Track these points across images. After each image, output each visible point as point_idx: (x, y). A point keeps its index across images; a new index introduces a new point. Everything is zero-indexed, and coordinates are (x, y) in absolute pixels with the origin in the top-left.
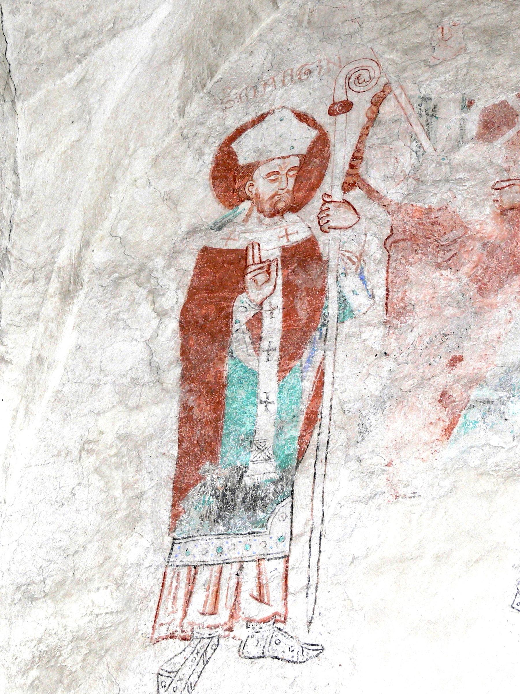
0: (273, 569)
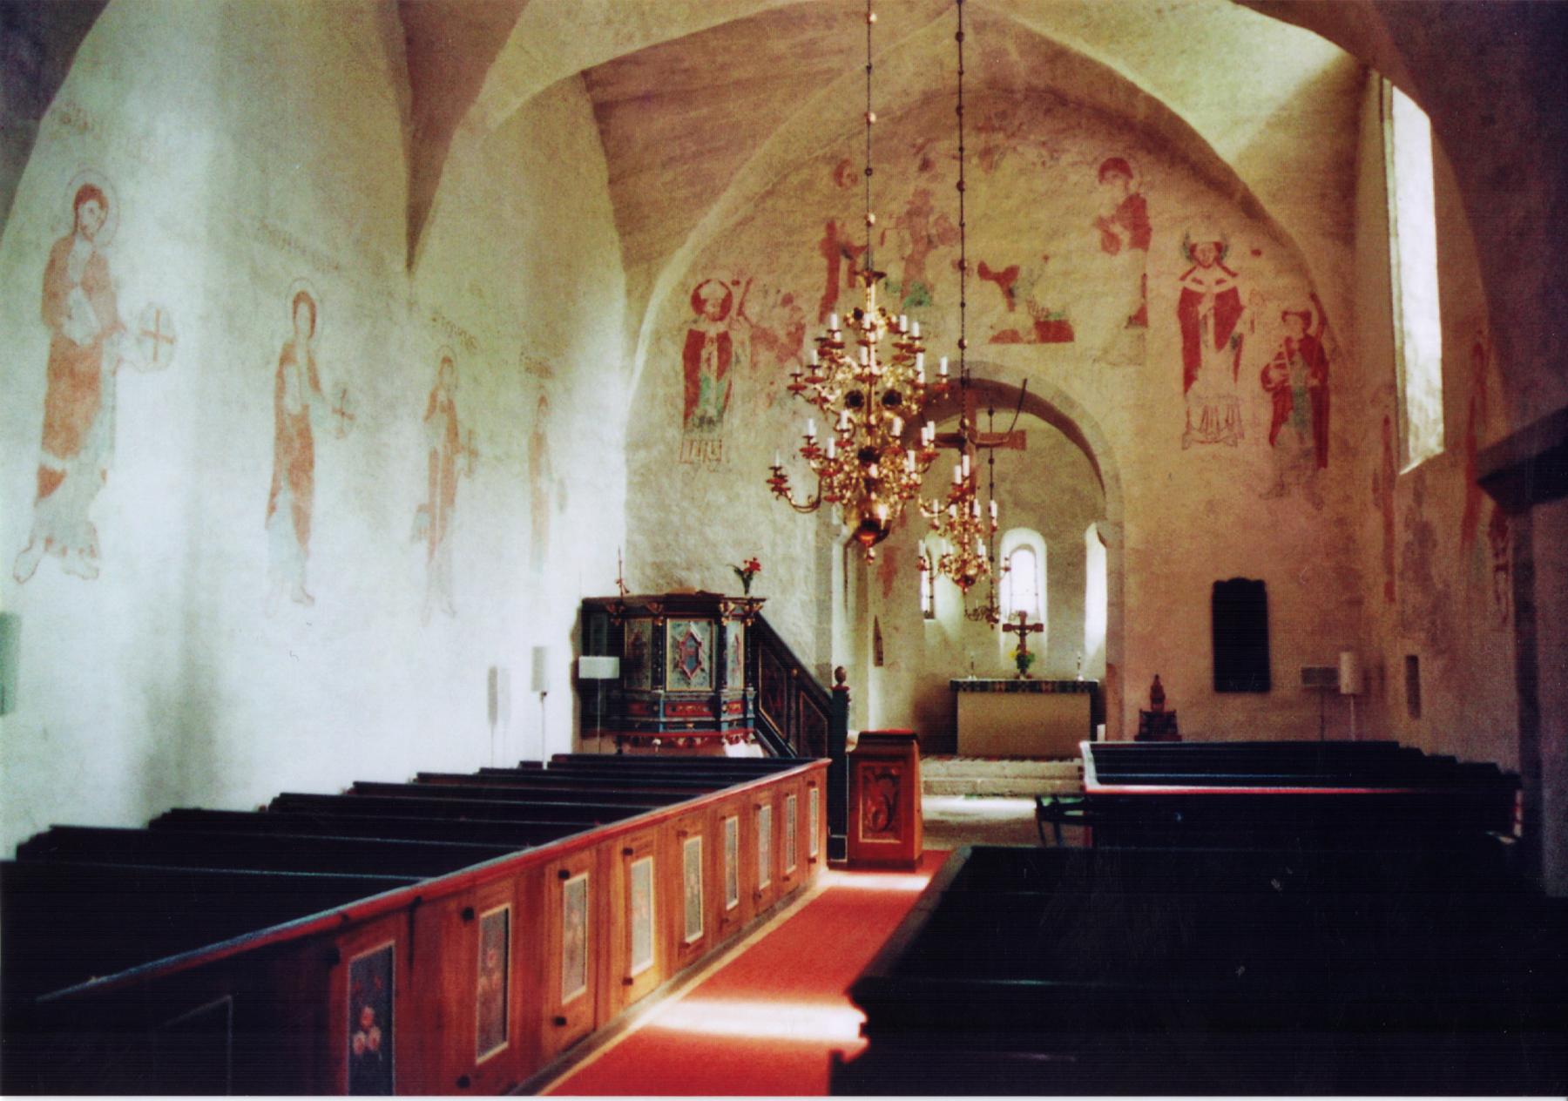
0: (716, 444)
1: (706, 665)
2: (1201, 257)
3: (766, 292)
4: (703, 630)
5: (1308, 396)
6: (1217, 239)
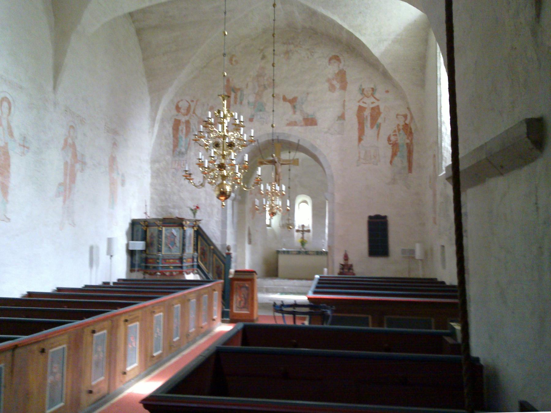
1: (178, 244)
2: (366, 94)
3: (204, 105)
4: (177, 231)
5: (405, 147)
6: (372, 86)
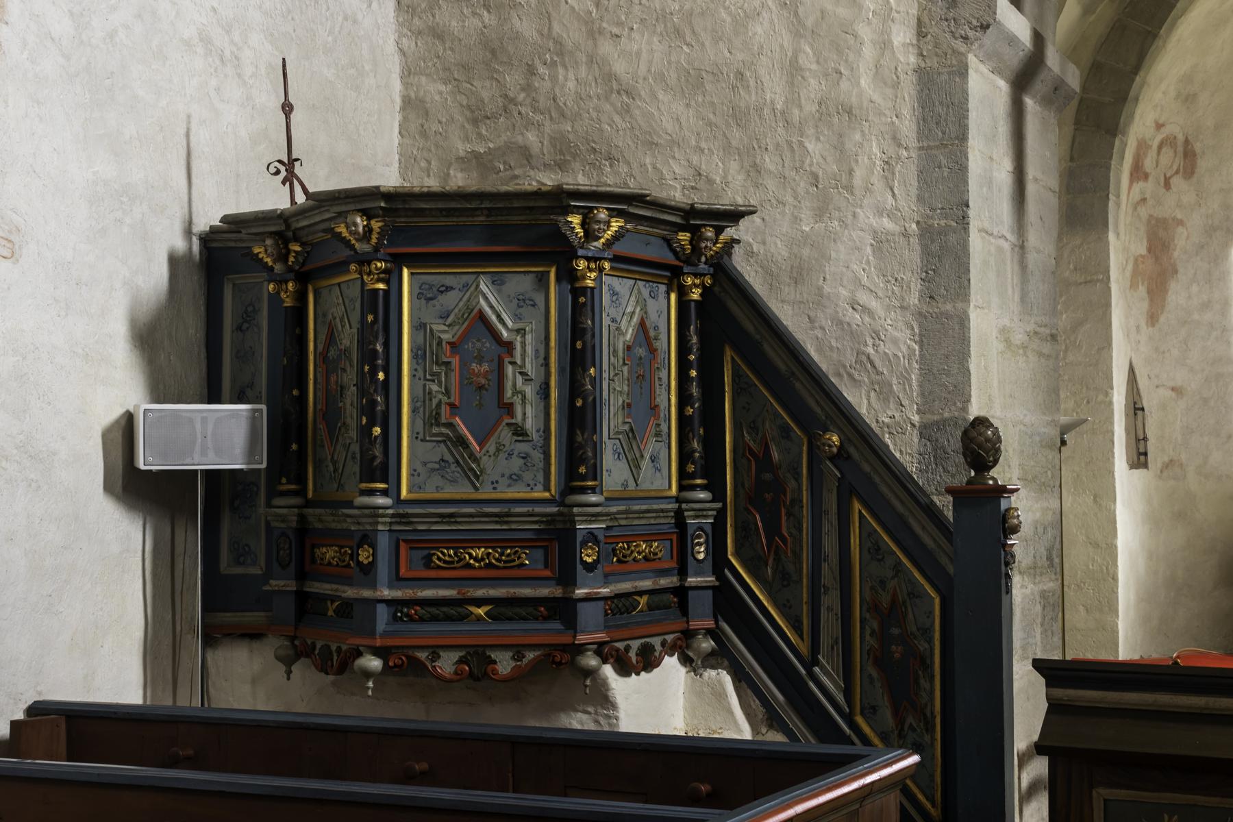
4: (522, 302)
